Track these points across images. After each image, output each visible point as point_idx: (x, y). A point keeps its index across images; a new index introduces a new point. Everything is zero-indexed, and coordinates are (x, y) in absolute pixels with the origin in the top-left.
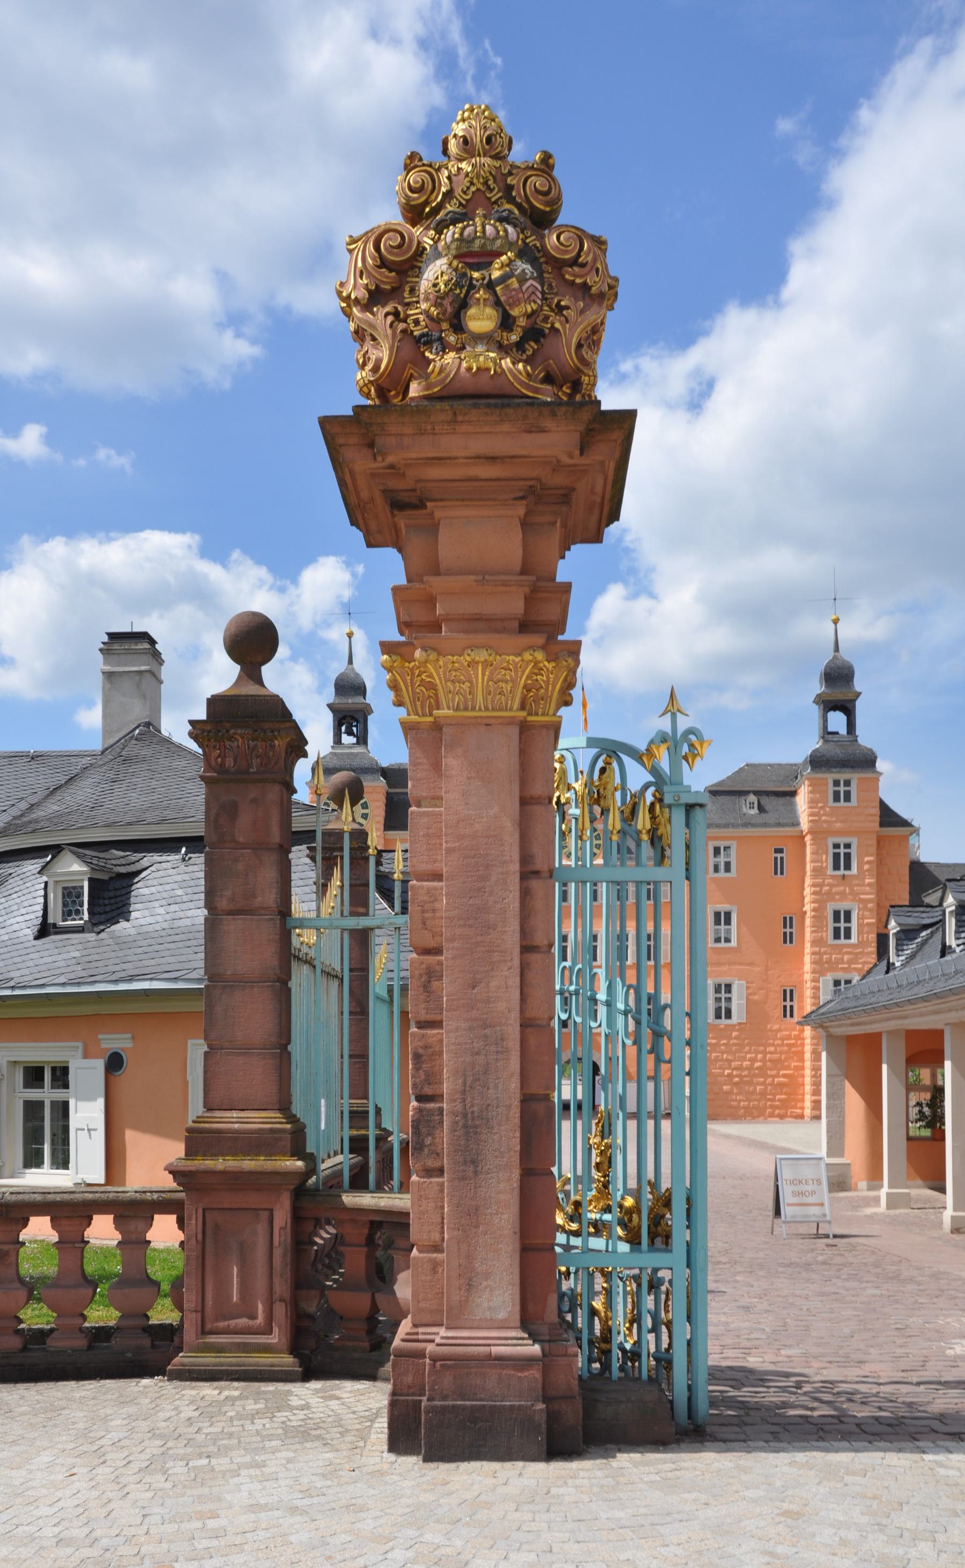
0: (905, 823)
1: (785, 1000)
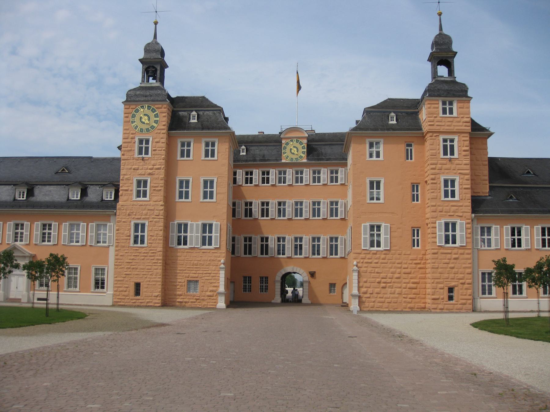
0: (483, 129)
1: (414, 236)
